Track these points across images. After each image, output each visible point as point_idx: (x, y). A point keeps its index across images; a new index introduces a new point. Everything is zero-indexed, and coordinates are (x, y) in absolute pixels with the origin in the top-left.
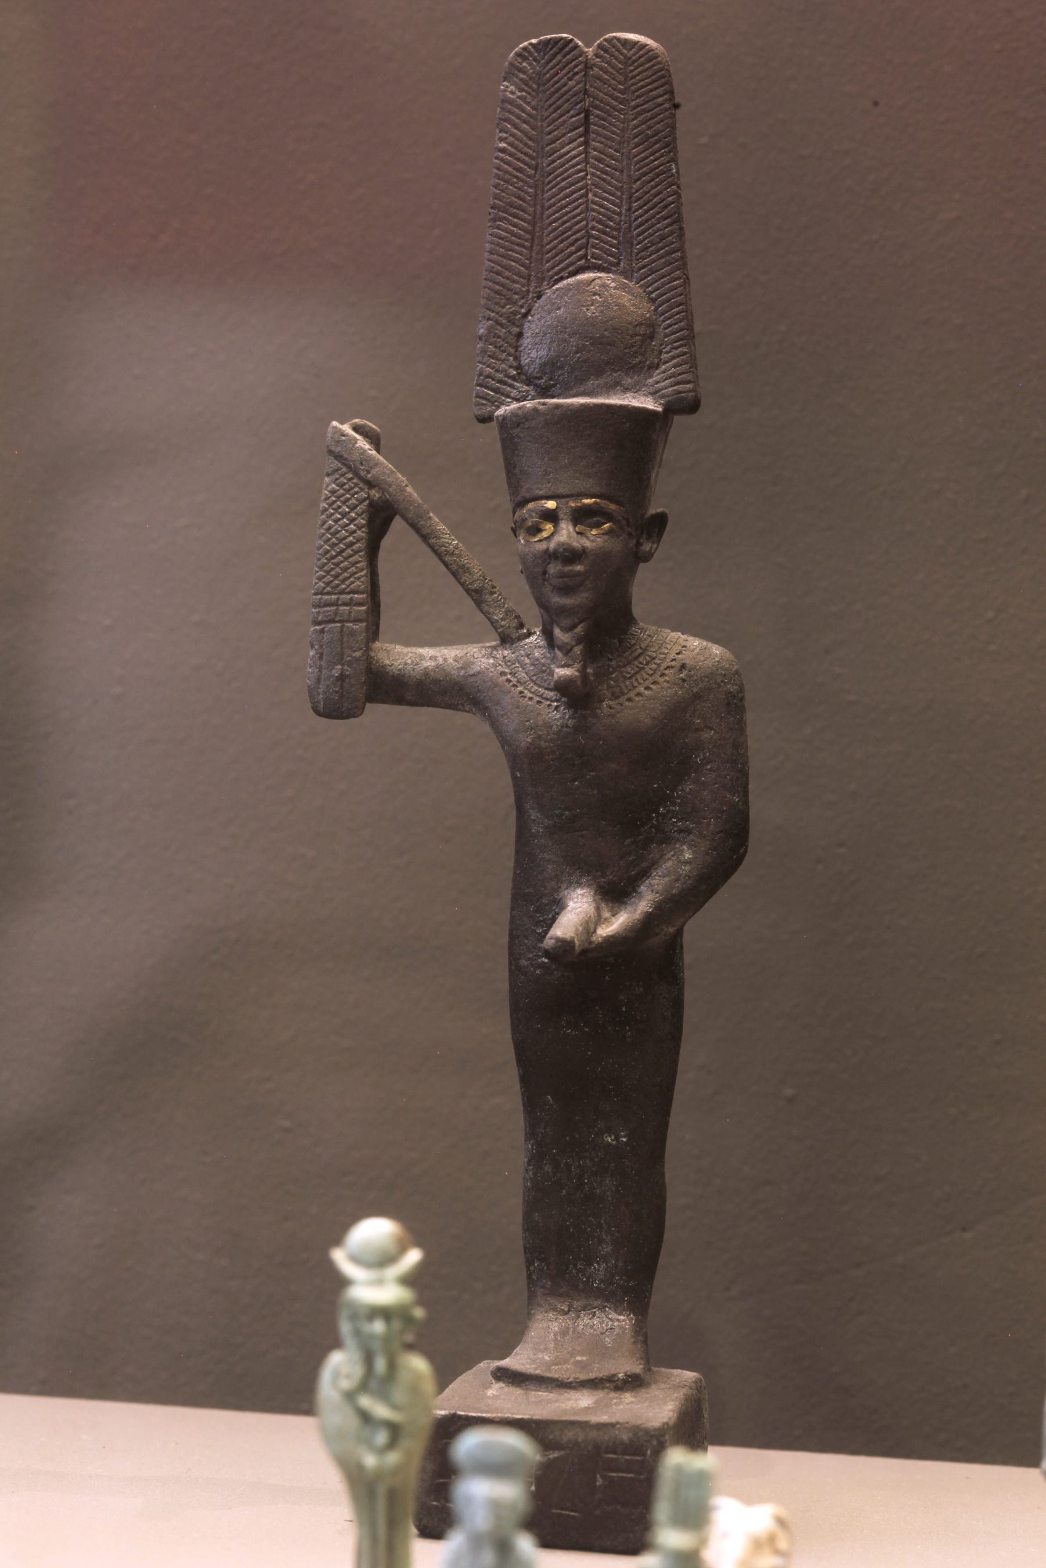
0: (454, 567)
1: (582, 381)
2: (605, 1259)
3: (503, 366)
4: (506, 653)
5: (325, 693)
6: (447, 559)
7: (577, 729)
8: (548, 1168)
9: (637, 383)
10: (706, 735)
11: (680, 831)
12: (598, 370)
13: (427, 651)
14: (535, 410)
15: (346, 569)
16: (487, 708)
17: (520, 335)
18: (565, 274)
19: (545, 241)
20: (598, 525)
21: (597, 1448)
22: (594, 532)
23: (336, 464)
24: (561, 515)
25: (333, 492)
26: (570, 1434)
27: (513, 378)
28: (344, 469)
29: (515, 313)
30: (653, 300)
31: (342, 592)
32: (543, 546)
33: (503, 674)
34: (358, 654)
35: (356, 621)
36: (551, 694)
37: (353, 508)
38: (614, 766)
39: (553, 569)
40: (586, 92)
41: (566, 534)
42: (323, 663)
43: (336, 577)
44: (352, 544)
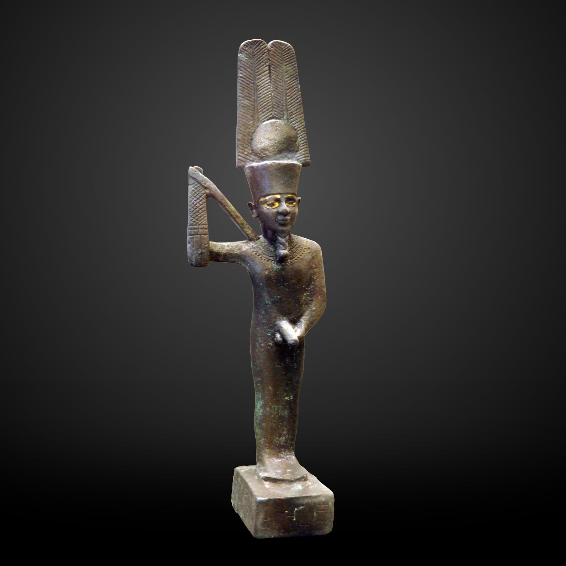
0: (234, 216)
1: (276, 155)
2: (285, 436)
3: (246, 150)
4: (253, 244)
5: (195, 258)
6: (232, 213)
7: (282, 269)
8: (268, 409)
9: (292, 157)
10: (316, 270)
11: (311, 301)
12: (280, 151)
13: (225, 244)
14: (271, 165)
15: (200, 217)
16: (249, 263)
17: (252, 139)
18: (265, 119)
19: (259, 108)
20: (292, 203)
21: (315, 504)
22: (291, 205)
23: (193, 181)
24: (282, 200)
25: (193, 191)
26: (306, 500)
27: (251, 154)
28: (196, 183)
29: (250, 132)
30: (295, 130)
31: (199, 225)
32: (275, 210)
33: (253, 251)
34: (207, 246)
35: (205, 234)
36: (271, 258)
37: (200, 197)
38: (293, 281)
39: (280, 218)
40: (269, 59)
41: (284, 206)
42: (194, 248)
43: (197, 219)
44: (201, 208)
